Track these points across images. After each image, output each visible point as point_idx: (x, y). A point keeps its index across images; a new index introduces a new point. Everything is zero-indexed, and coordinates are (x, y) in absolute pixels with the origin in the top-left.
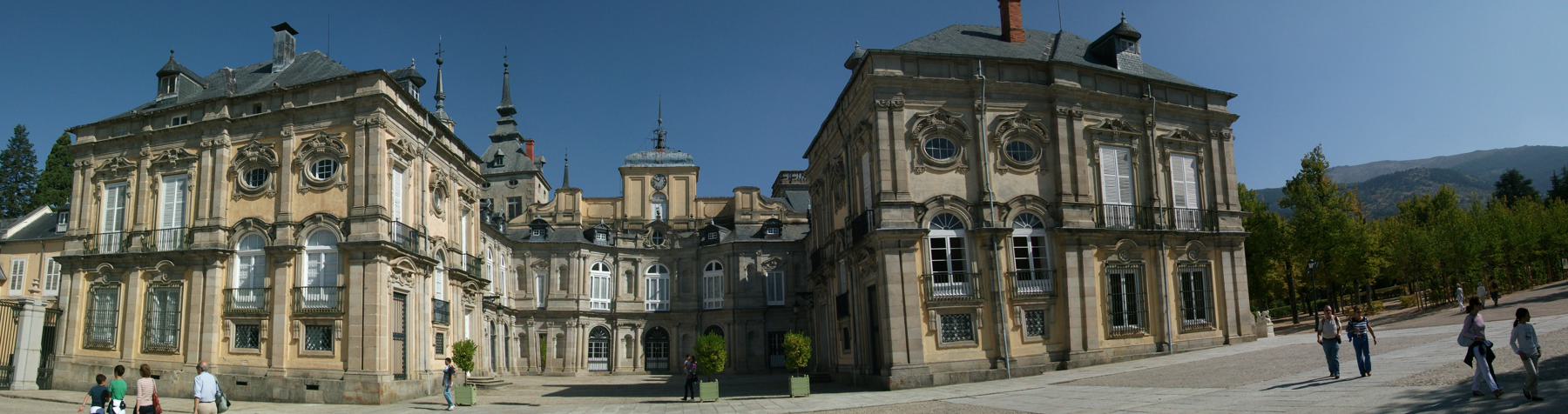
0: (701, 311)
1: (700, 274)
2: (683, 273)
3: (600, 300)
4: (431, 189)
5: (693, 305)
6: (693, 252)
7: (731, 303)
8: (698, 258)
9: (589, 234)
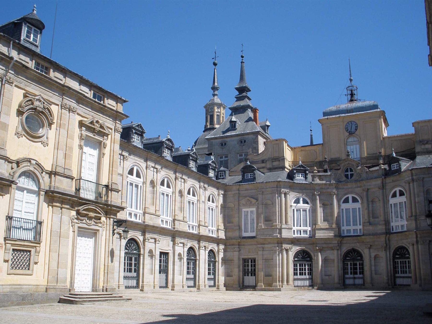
0: (388, 232)
1: (385, 201)
2: (369, 201)
3: (302, 228)
4: (20, 113)
5: (381, 228)
6: (379, 182)
7: (413, 225)
8: (383, 187)
9: (291, 176)
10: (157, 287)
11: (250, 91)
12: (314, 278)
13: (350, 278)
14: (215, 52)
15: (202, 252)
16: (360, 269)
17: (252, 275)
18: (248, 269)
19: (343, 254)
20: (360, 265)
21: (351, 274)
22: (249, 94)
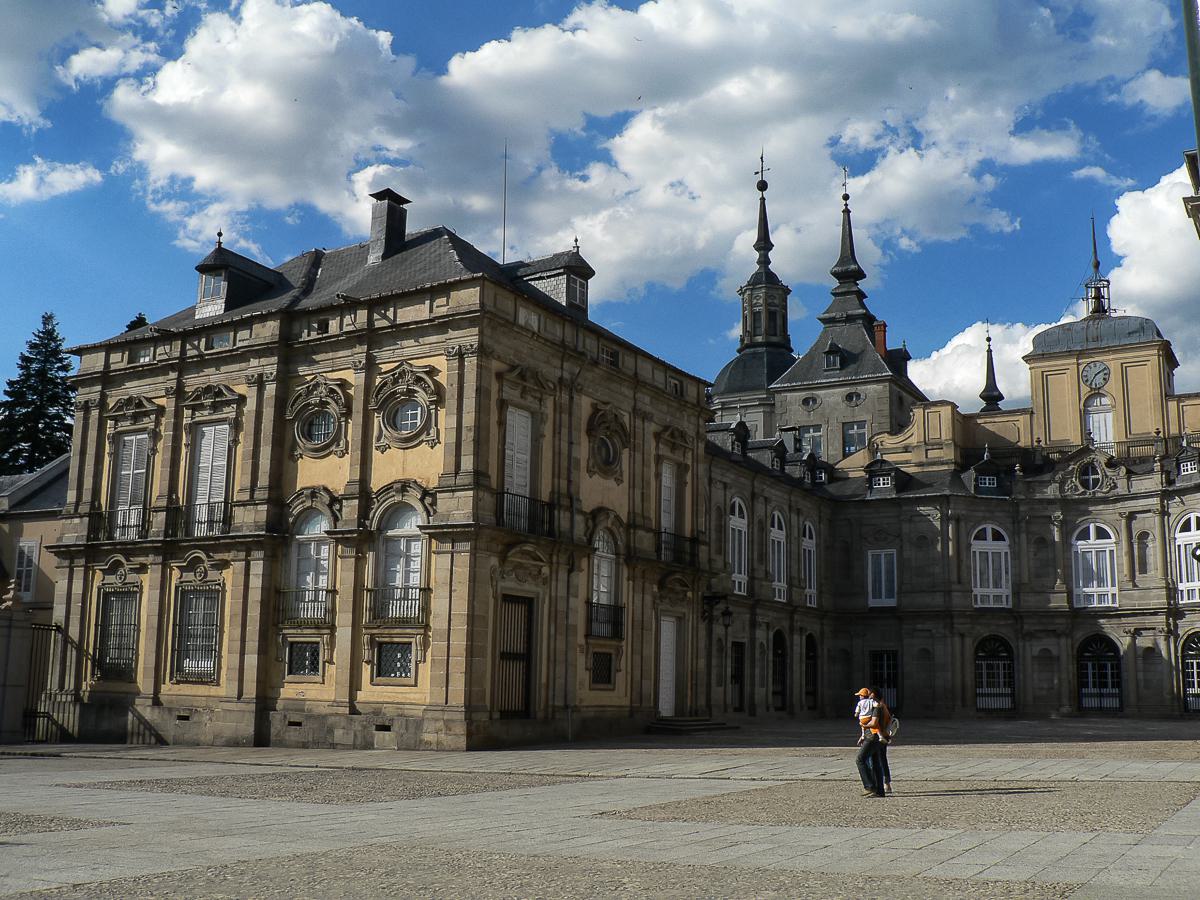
1: (1166, 542)
10: (730, 710)
11: (864, 276)
12: (1016, 692)
13: (1091, 695)
14: (762, 158)
15: (796, 638)
16: (1112, 677)
17: (889, 687)
18: (882, 675)
19: (1077, 645)
20: (1112, 669)
21: (1094, 686)
22: (862, 285)
